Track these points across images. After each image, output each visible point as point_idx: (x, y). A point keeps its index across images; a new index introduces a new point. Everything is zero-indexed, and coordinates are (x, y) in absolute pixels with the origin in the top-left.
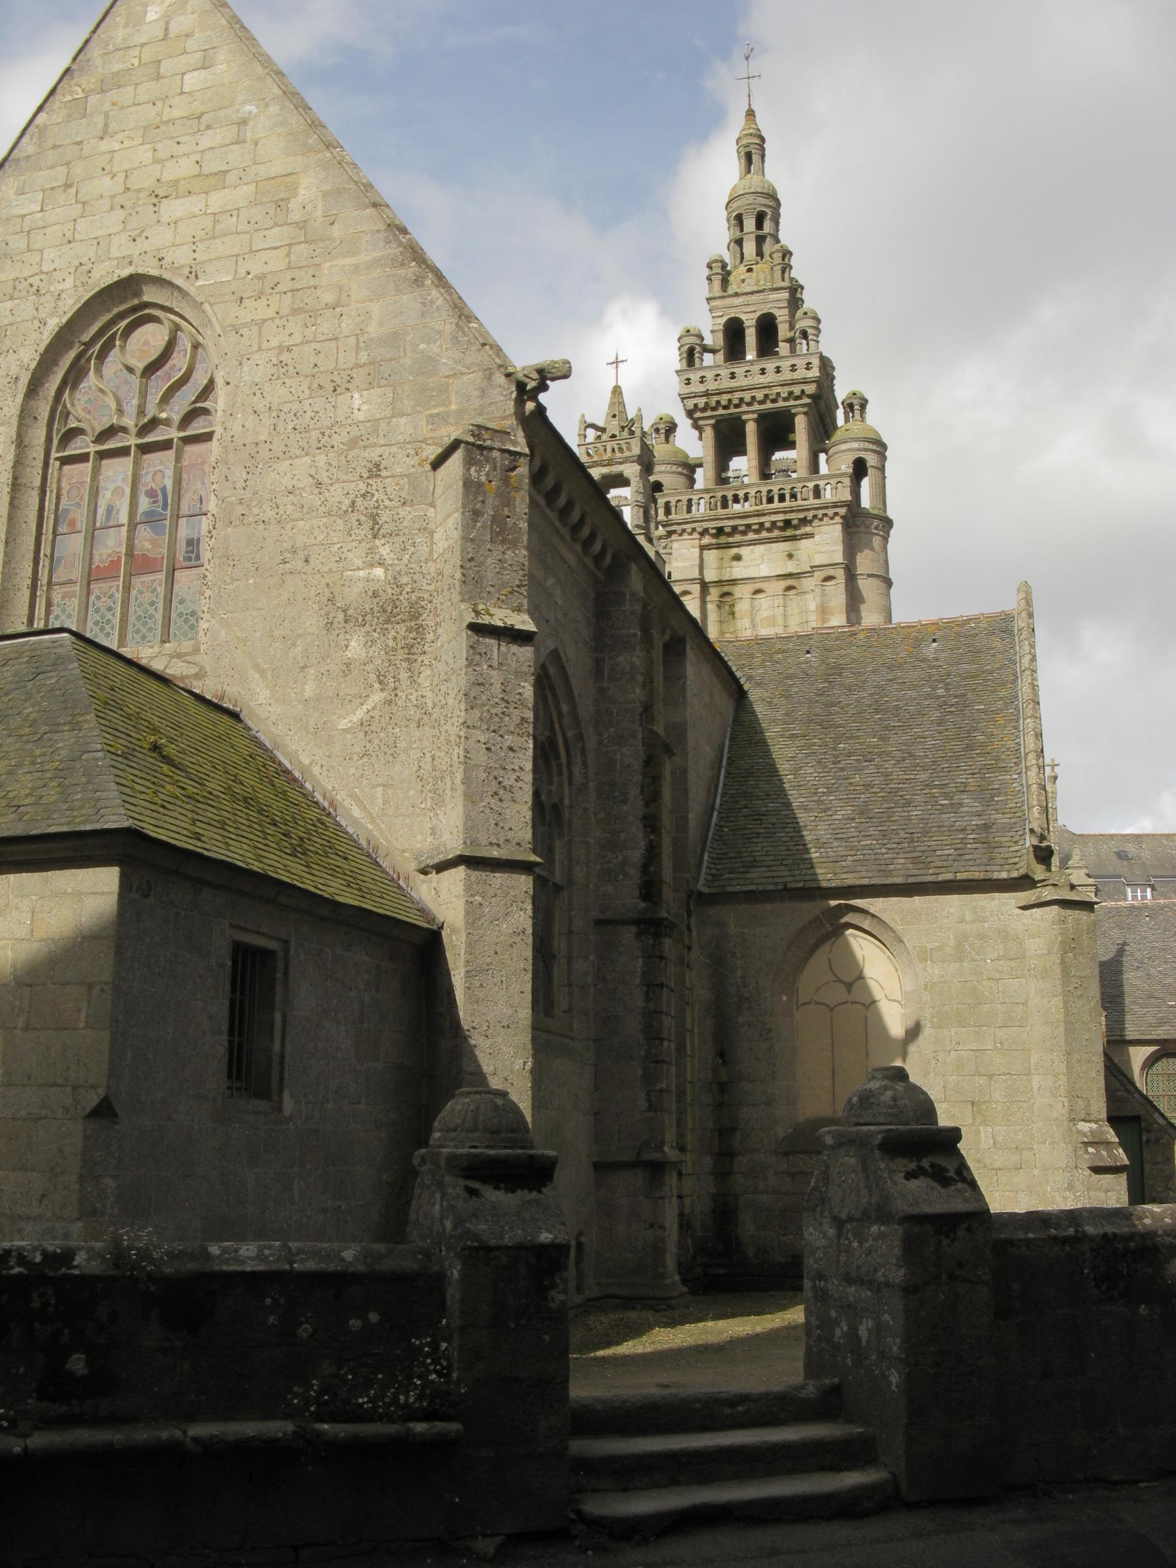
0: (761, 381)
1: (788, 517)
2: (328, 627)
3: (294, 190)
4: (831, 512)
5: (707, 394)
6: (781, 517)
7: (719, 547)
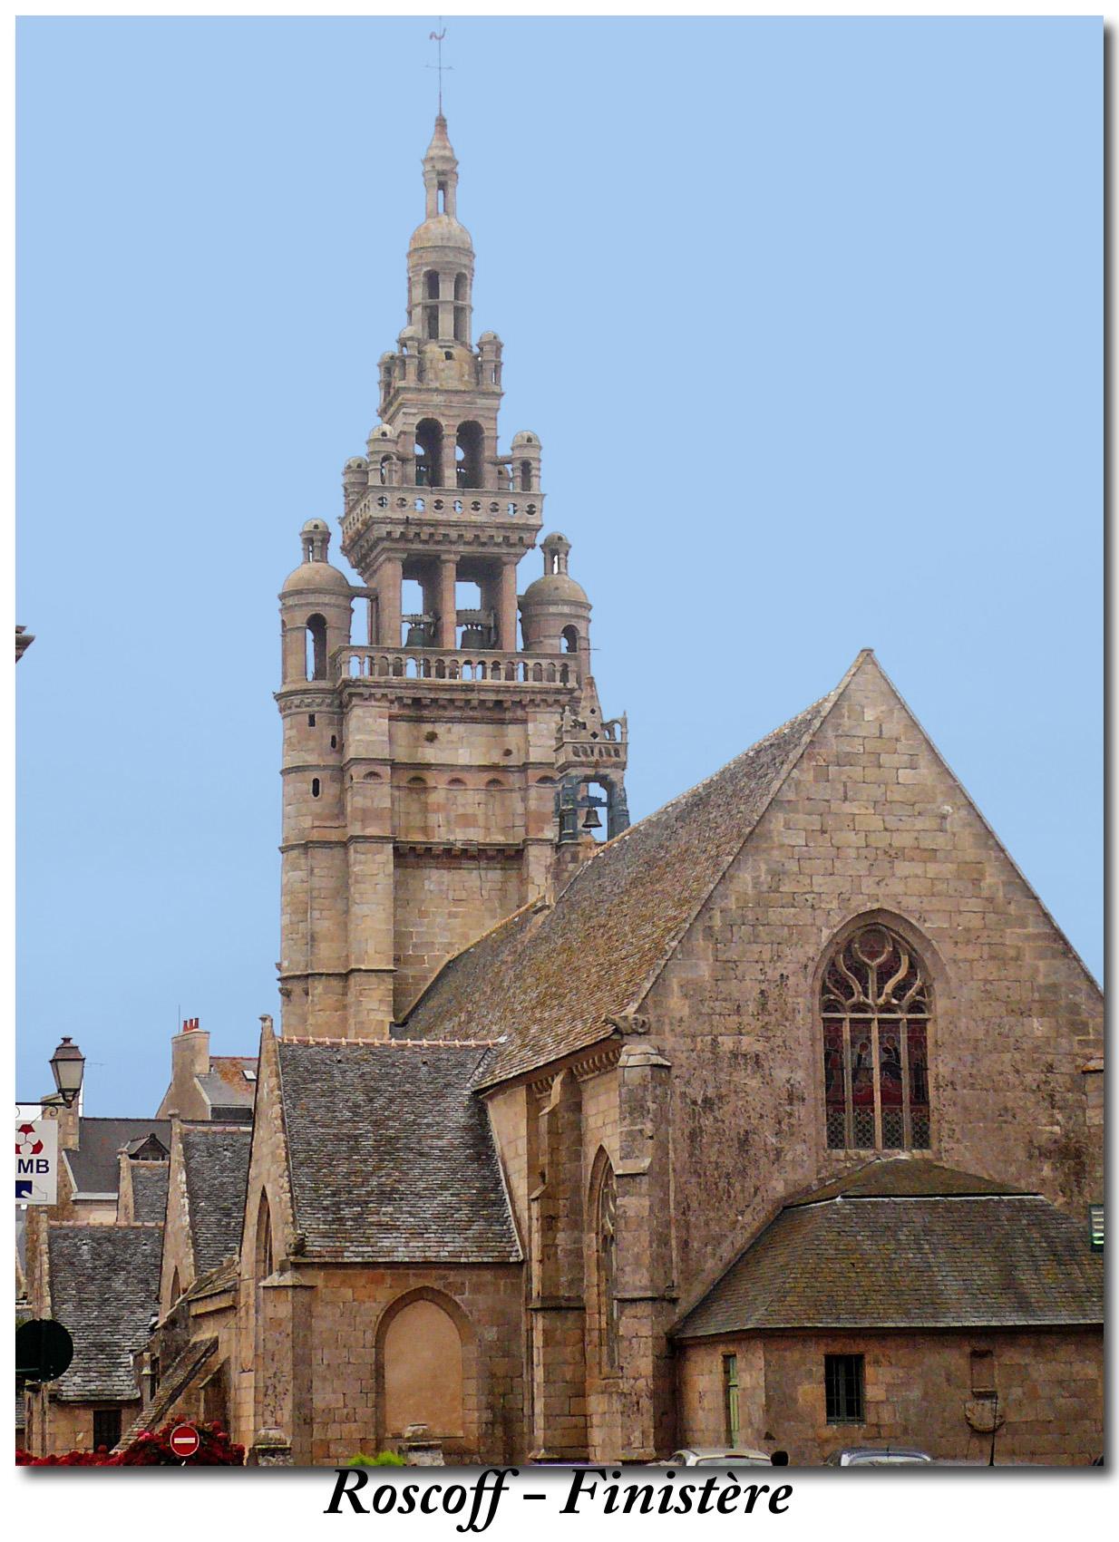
0: (473, 518)
1: (500, 697)
2: (1031, 1157)
3: (982, 874)
4: (551, 699)
5: (407, 522)
6: (493, 697)
7: (409, 719)
